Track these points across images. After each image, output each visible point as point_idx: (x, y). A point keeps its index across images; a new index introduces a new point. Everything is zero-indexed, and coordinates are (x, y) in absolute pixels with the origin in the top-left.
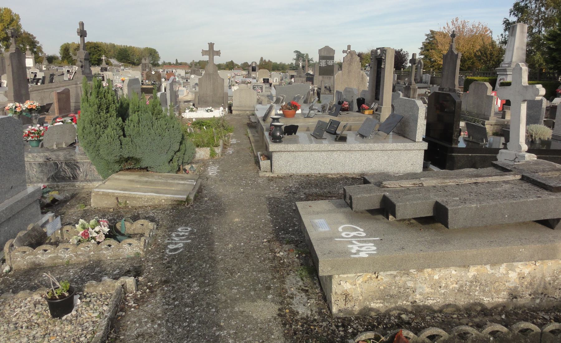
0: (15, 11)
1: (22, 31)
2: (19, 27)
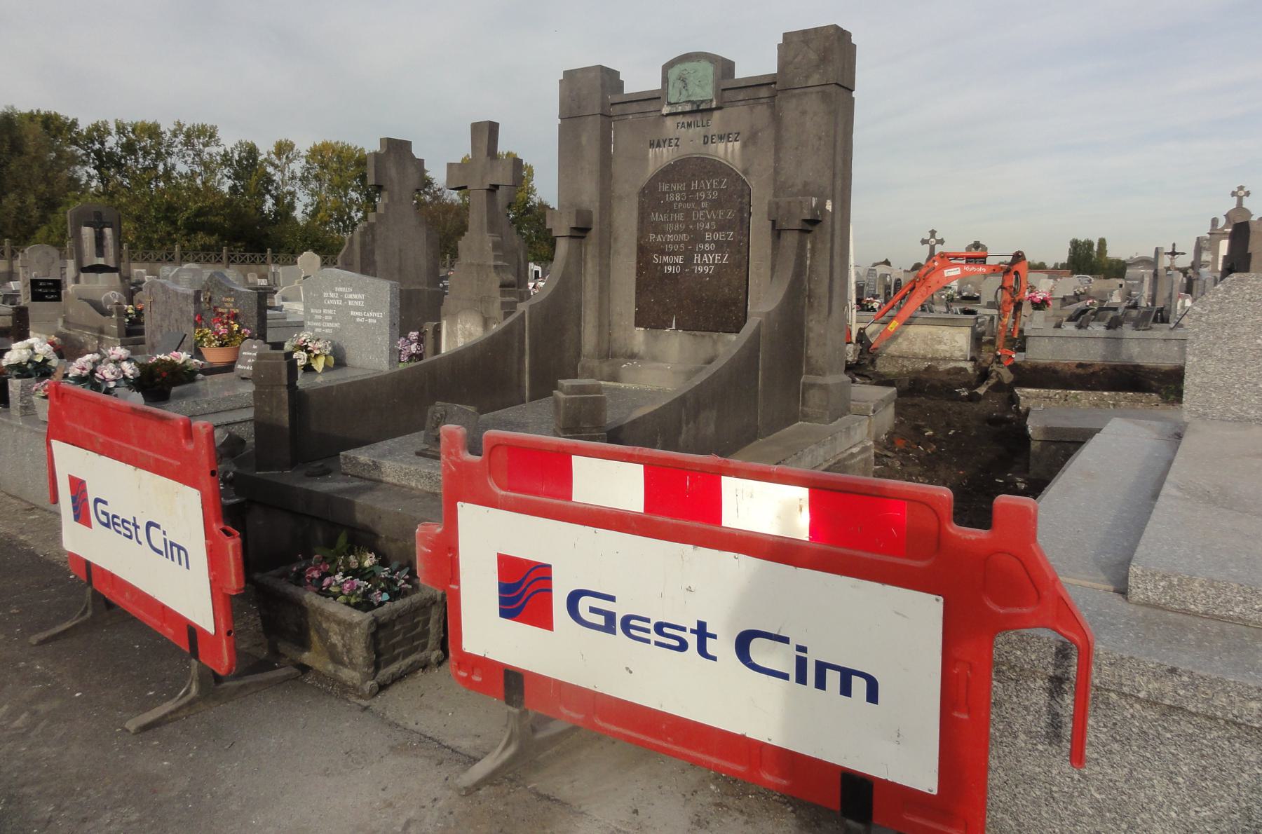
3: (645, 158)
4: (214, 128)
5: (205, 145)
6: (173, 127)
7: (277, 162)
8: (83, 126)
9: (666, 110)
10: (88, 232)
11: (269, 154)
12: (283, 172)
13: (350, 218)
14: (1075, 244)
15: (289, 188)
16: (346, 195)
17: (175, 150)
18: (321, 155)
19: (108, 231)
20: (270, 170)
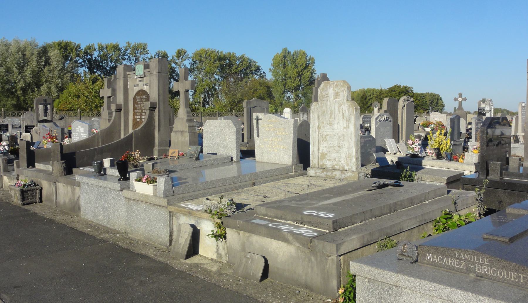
0: (309, 54)
3: (134, 90)
4: (145, 45)
6: (125, 45)
7: (177, 61)
8: (83, 47)
9: (136, 77)
10: (41, 107)
11: (173, 57)
12: (180, 66)
13: (215, 90)
17: (126, 57)
19: (48, 106)
20: (173, 65)
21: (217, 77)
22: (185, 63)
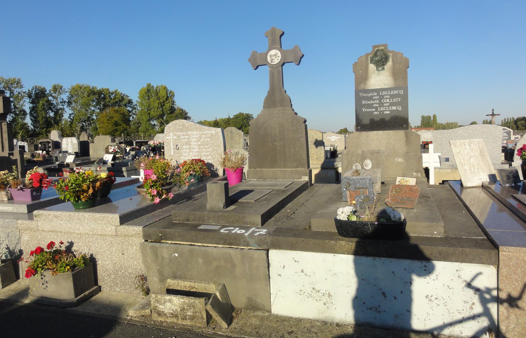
0: (169, 88)
1: (176, 107)
2: (173, 102)
4: (19, 80)
5: (15, 88)
7: (54, 95)
14: (423, 118)
15: (60, 106)
16: (90, 109)
18: (76, 91)
20: (50, 98)
21: (93, 108)
22: (62, 96)
